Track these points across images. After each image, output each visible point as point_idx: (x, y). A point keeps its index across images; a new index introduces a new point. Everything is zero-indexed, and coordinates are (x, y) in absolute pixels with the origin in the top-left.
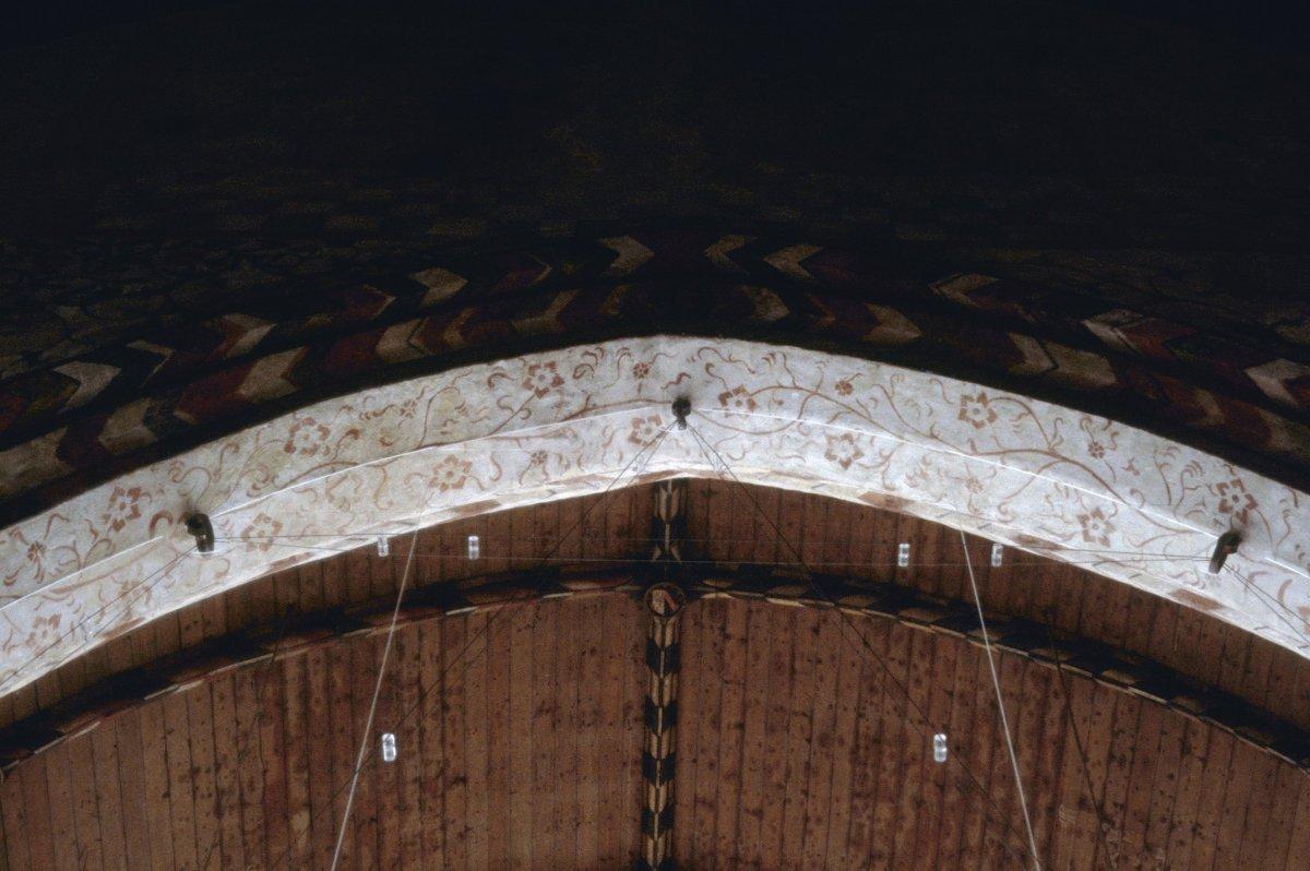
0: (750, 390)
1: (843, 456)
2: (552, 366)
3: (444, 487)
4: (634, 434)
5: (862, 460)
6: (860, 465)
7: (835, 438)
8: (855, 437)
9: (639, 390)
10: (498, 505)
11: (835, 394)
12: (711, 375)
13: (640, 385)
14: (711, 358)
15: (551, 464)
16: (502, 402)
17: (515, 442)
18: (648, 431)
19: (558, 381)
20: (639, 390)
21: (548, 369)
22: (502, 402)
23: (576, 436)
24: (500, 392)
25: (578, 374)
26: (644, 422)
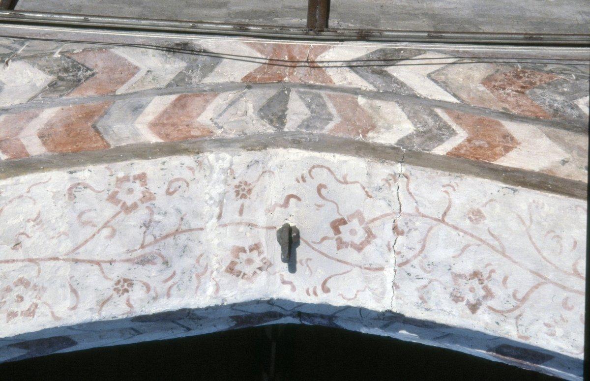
0: (367, 216)
1: (471, 298)
3: (12, 315)
4: (233, 263)
6: (491, 308)
7: (460, 276)
8: (486, 275)
9: (241, 212)
10: (74, 343)
12: (323, 198)
13: (242, 206)
14: (322, 176)
16: (85, 218)
17: (96, 267)
18: (249, 261)
19: (148, 197)
20: (241, 212)
21: (138, 182)
22: (85, 218)
23: (166, 263)
24: (81, 206)
25: (171, 190)
26: (245, 251)
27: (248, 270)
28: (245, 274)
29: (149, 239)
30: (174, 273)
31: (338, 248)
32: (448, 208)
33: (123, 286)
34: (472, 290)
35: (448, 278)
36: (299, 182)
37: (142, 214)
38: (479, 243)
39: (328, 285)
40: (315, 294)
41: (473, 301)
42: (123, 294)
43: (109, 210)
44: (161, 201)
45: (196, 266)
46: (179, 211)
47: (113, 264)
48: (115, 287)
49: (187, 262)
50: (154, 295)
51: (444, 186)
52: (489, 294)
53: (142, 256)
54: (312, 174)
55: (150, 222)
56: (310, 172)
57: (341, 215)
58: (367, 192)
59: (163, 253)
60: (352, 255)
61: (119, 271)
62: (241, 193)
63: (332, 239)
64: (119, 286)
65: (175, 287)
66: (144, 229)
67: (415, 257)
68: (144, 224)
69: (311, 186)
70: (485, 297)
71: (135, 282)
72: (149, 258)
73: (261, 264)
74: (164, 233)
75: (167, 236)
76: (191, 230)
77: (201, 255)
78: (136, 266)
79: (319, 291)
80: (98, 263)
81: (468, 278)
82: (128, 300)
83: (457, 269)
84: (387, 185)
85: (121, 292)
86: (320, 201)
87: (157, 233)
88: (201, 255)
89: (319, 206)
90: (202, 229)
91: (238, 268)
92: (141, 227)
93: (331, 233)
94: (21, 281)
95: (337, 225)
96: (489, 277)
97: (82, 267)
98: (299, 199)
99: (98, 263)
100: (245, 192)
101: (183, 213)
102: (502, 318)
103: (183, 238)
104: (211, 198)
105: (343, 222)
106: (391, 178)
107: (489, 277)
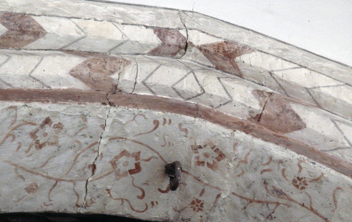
0: (113, 176)
1: (48, 129)
5: (34, 128)
7: (52, 144)
9: (203, 191)
11: (40, 180)
15: (292, 172)
20: (203, 191)
23: (265, 183)
26: (208, 164)
27: (208, 150)
28: (213, 148)
29: (272, 207)
30: (262, 173)
31: (139, 153)
32: (51, 190)
33: (300, 184)
34: (45, 135)
35: (63, 140)
36: (157, 202)
38: (34, 171)
39: (154, 126)
40: (165, 120)
41: (47, 125)
42: (302, 178)
45: (245, 170)
46: (246, 214)
47: (302, 203)
48: (306, 187)
49: (251, 176)
50: (281, 165)
51: (51, 204)
52: (33, 135)
53: (281, 198)
54: (145, 207)
55: (268, 218)
56: (147, 209)
57: (132, 177)
58: (109, 193)
59: (264, 191)
60: (131, 148)
61: (297, 196)
62: (199, 204)
63: (143, 160)
64: (303, 185)
65: (265, 162)
66: (273, 215)
67: (83, 151)
68: (272, 218)
69: (147, 200)
70: (37, 131)
71: (291, 182)
72: (275, 193)
73: (199, 150)
74: (260, 204)
75: (259, 202)
76: (241, 197)
77: (239, 176)
78: (286, 193)
79: (161, 121)
80: (312, 209)
81: (47, 143)
82: (300, 171)
83: (54, 148)
84: (93, 200)
85: (302, 180)
86: (144, 187)
87: (265, 209)
88: (239, 176)
89: (146, 184)
90: (233, 194)
91: (216, 155)
92: (275, 217)
93: (142, 164)
96: (30, 147)
97: (323, 213)
98: (160, 190)
99: (312, 209)
100: (197, 204)
101: (243, 211)
102: (26, 119)
103: (248, 195)
104: (221, 211)
105: (131, 172)
106: (89, 205)
107: (30, 147)
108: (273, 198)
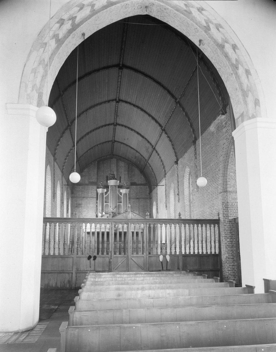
1: (127, 5)
2: (161, 19)
35: (129, 6)
37: (162, 15)
43: (165, 18)
44: (159, 15)
49: (158, 8)
60: (140, 5)
94: (175, 17)
95: (141, 7)
108: (162, 11)
